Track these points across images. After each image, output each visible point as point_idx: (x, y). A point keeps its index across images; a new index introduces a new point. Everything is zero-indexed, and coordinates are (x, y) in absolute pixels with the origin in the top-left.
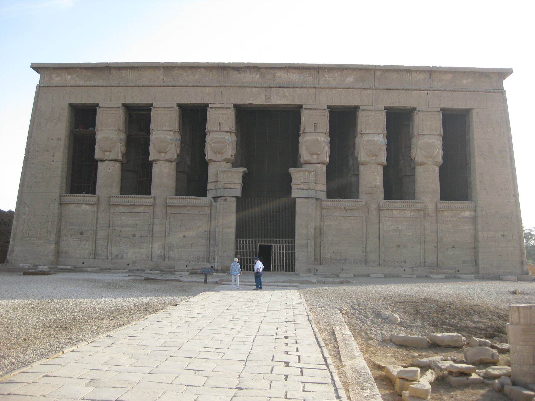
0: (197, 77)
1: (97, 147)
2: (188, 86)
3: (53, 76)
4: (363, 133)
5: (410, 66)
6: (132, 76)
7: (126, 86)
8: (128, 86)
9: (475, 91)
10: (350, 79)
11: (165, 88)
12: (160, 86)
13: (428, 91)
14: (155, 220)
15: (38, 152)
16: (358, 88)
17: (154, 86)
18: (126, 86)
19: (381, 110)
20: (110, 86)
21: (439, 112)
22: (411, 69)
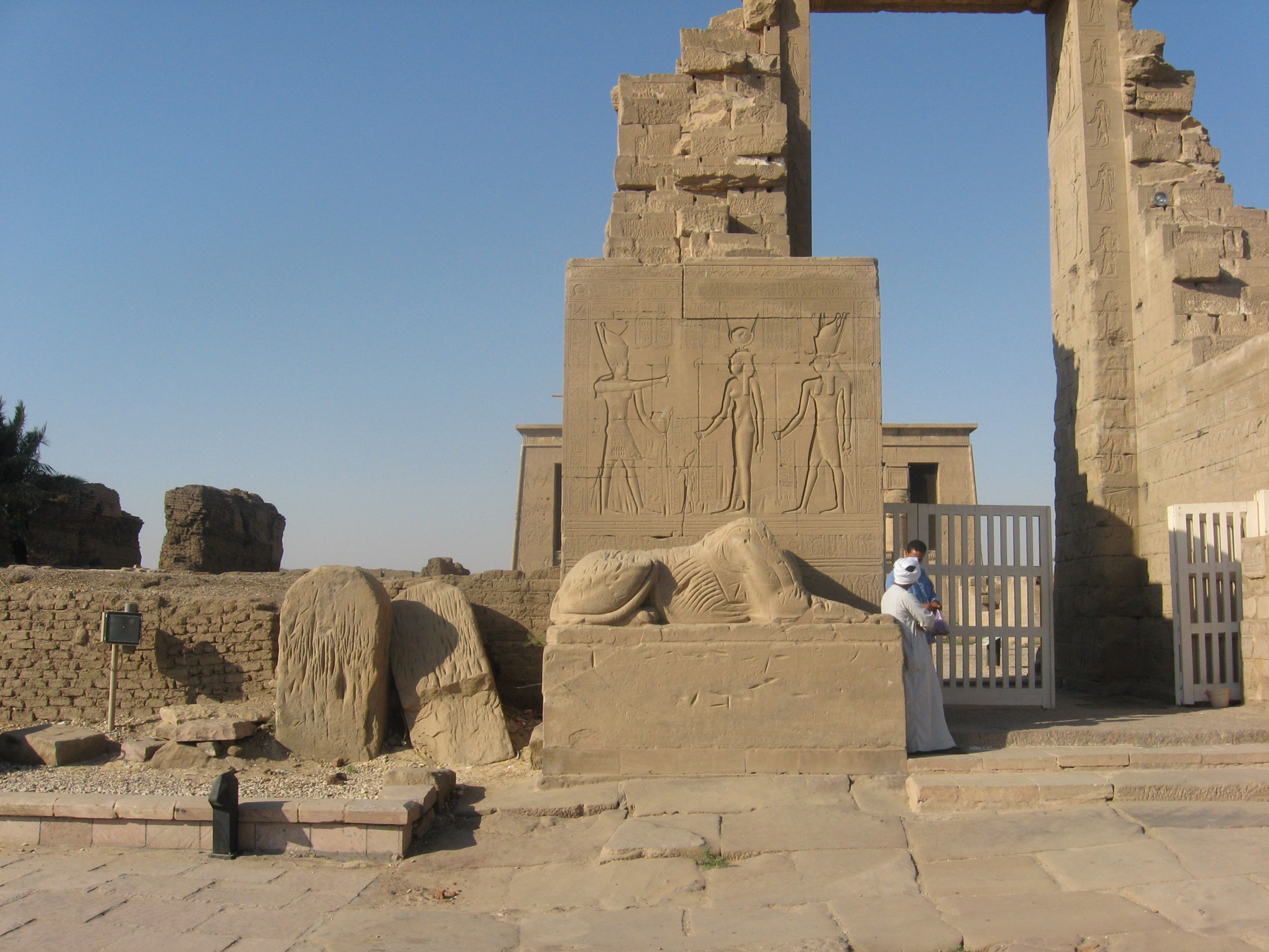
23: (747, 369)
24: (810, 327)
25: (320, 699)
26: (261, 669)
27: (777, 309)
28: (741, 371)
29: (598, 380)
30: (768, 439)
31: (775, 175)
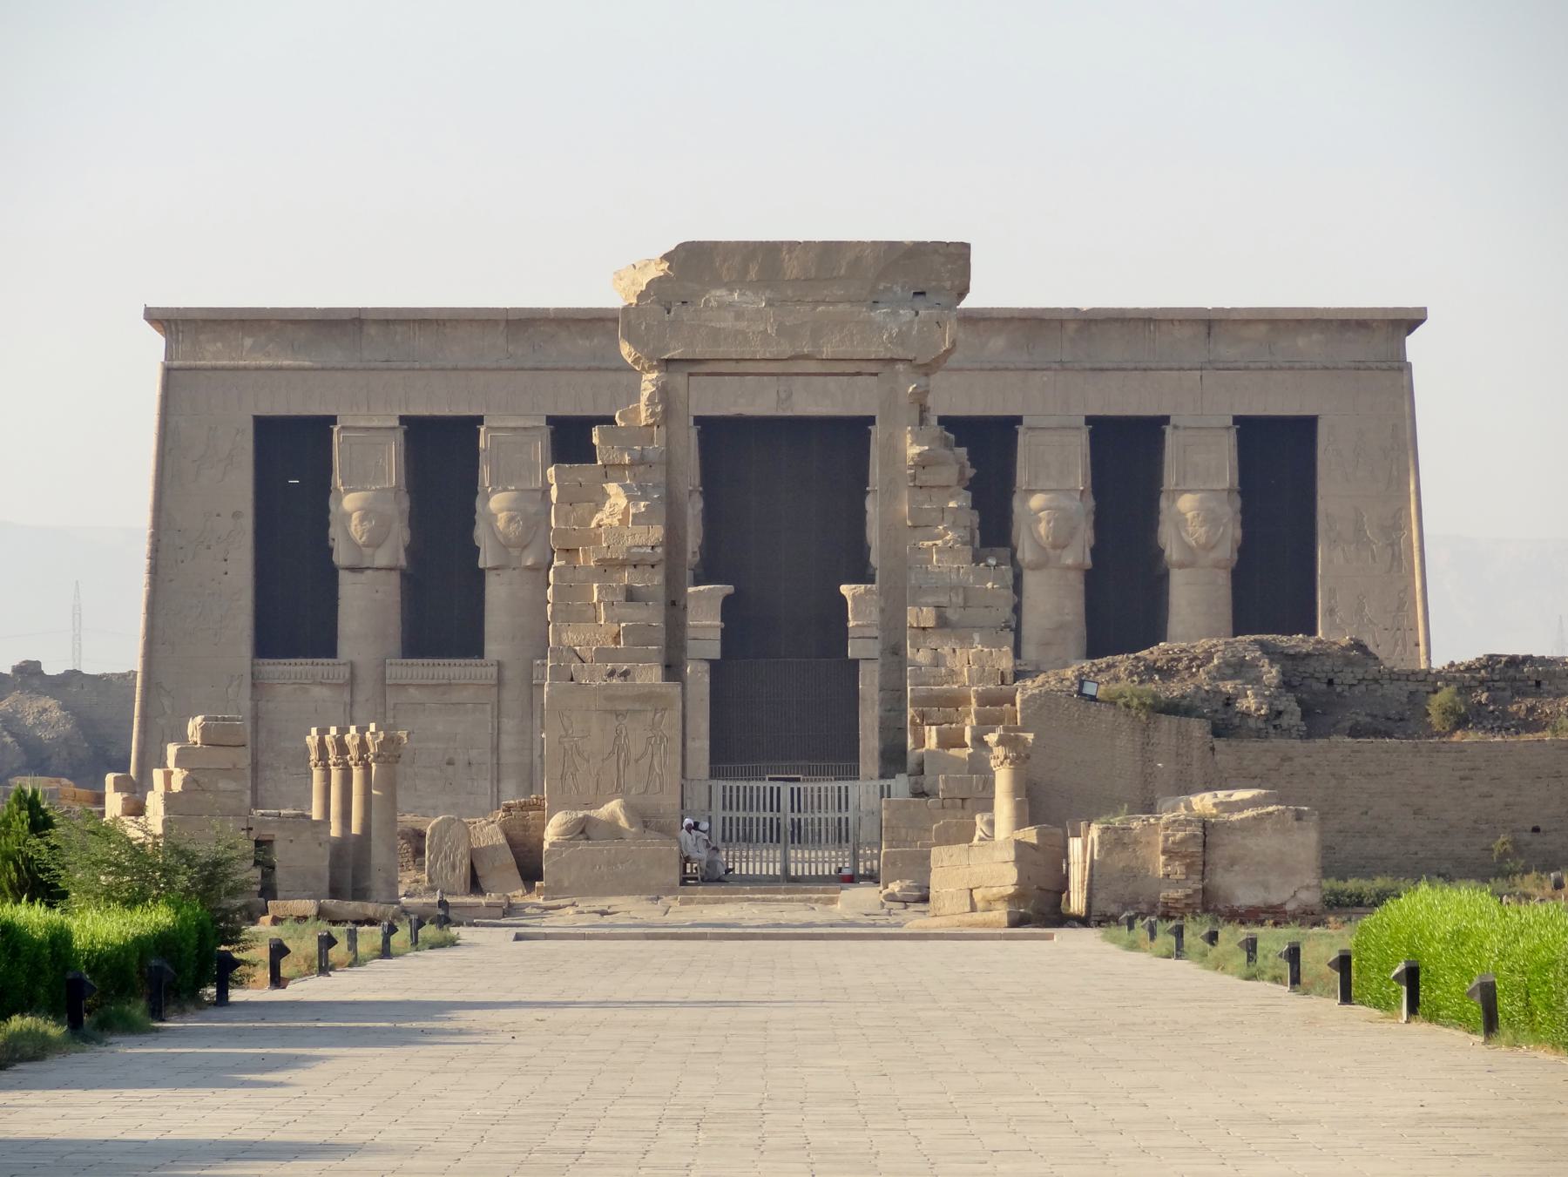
0: (596, 341)
1: (334, 531)
2: (573, 369)
3: (202, 337)
4: (1031, 490)
5: (1155, 310)
6: (422, 339)
7: (409, 369)
8: (414, 369)
9: (1326, 368)
10: (997, 344)
11: (513, 372)
12: (500, 369)
13: (1204, 372)
14: (505, 720)
15: (182, 548)
16: (1018, 369)
17: (485, 369)
18: (409, 369)
19: (1078, 428)
20: (364, 369)
21: (1228, 428)
22: (1154, 317)
23: (624, 732)
24: (650, 715)
25: (444, 872)
26: (408, 861)
27: (637, 706)
28: (621, 732)
29: (561, 737)
30: (632, 762)
31: (653, 560)
